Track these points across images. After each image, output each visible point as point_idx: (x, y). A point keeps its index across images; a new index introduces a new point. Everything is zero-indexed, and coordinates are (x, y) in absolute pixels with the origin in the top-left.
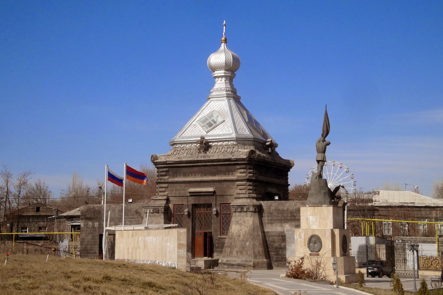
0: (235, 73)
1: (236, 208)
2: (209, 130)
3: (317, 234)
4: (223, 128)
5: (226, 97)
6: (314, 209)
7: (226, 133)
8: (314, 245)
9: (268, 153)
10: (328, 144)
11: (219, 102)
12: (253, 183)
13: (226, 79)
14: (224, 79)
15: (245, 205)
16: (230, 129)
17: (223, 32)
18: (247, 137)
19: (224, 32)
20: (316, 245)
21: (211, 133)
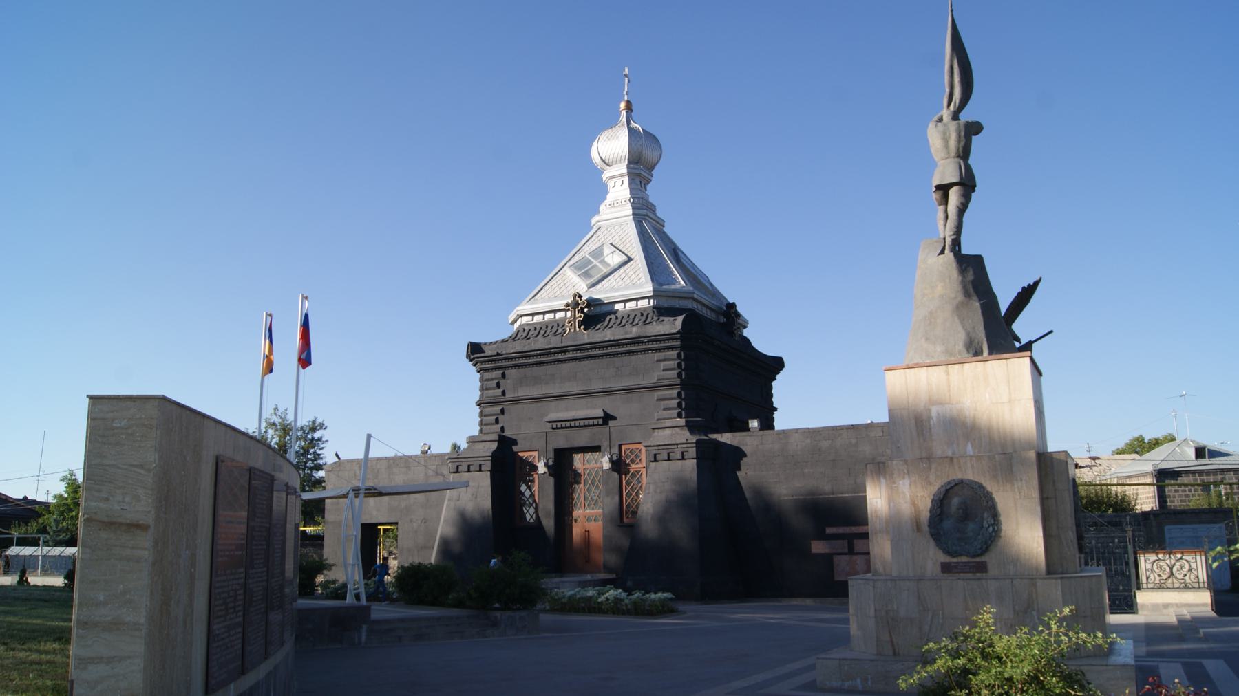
0: (652, 172)
1: (655, 452)
4: (622, 277)
6: (947, 373)
14: (626, 180)
17: (624, 90)
19: (626, 89)
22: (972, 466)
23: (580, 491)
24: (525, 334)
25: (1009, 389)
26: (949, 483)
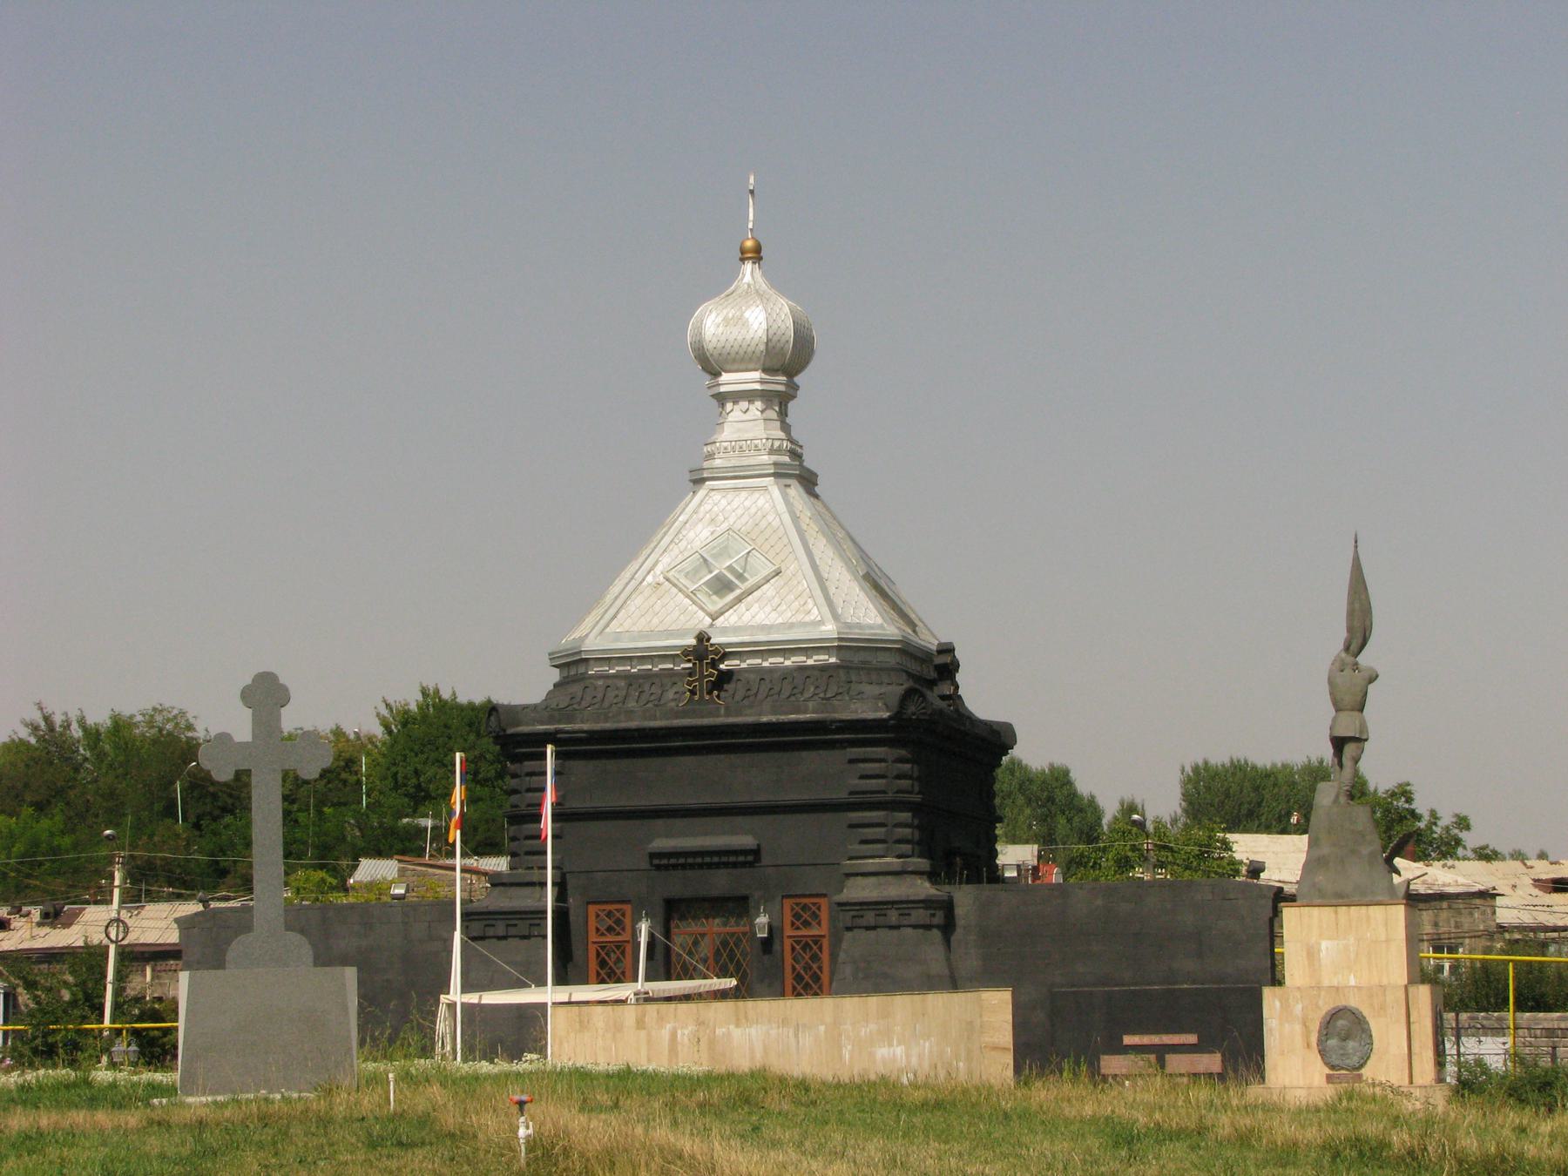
2: (723, 610)
3: (1353, 1005)
4: (777, 600)
6: (1336, 912)
7: (794, 620)
8: (1344, 1044)
9: (939, 696)
10: (1373, 678)
11: (744, 494)
12: (913, 816)
15: (893, 902)
16: (810, 603)
18: (879, 635)
20: (1351, 1044)
21: (730, 618)
22: (1354, 995)
24: (600, 696)
25: (1387, 930)
26: (1334, 1009)
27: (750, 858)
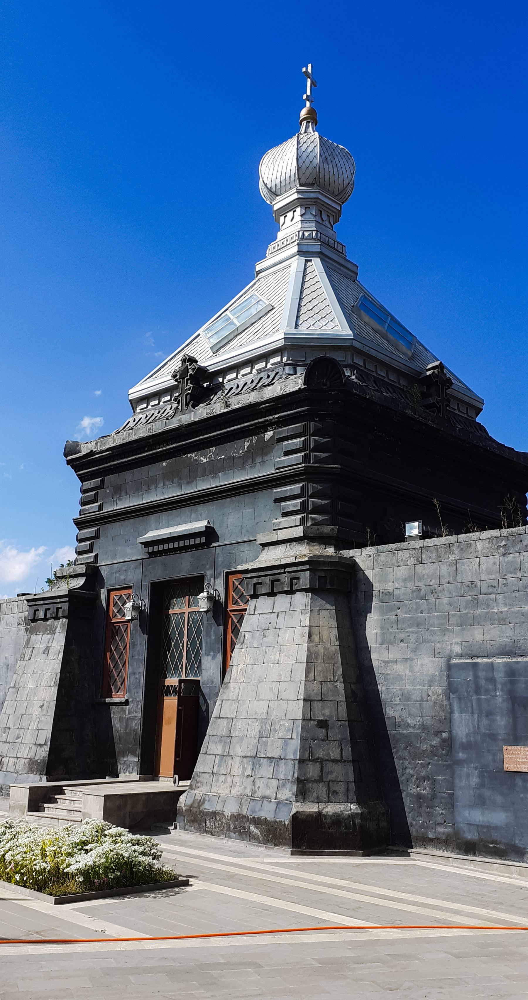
1: (255, 581)
5: (298, 256)
13: (304, 211)
23: (183, 646)
27: (203, 540)
